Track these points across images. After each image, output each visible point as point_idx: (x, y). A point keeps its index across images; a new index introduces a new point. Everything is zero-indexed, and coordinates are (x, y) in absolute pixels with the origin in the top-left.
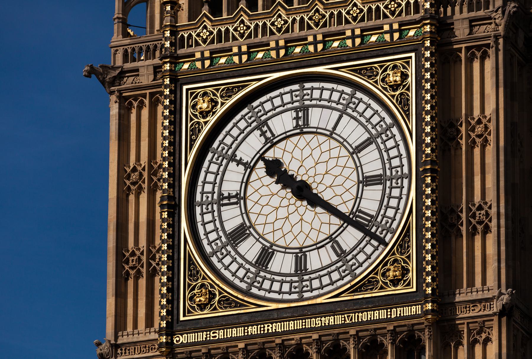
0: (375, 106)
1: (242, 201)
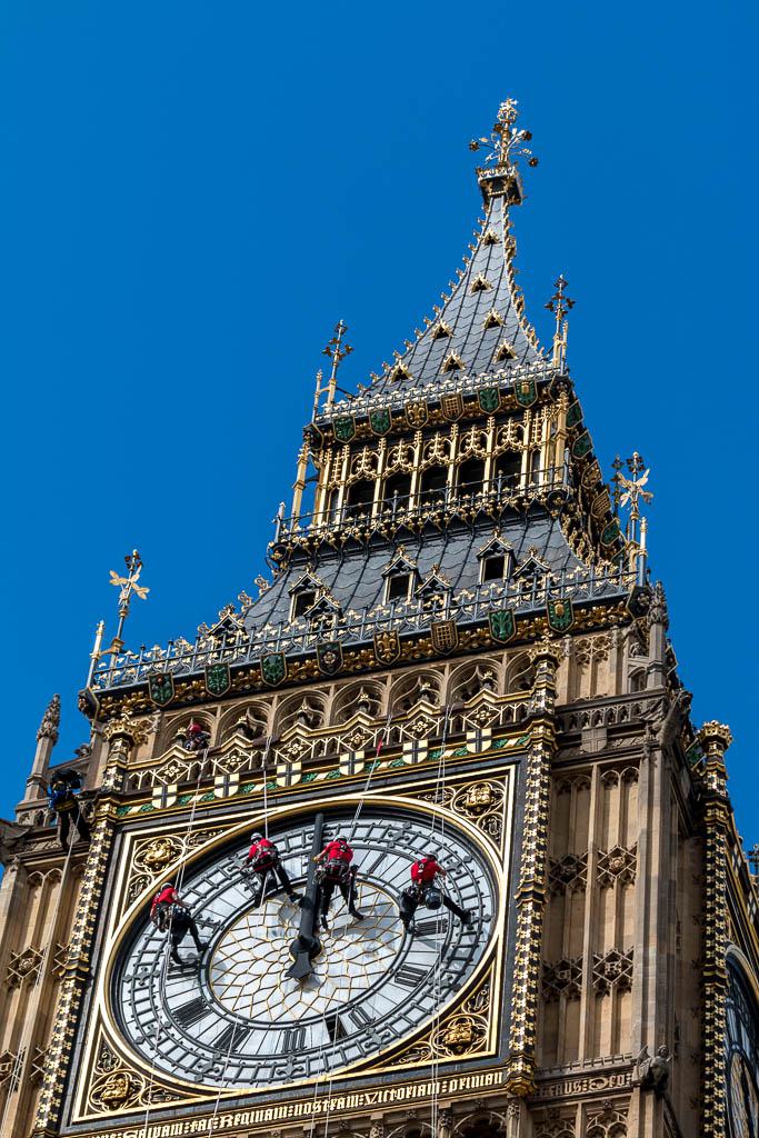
0: (440, 838)
1: (203, 971)
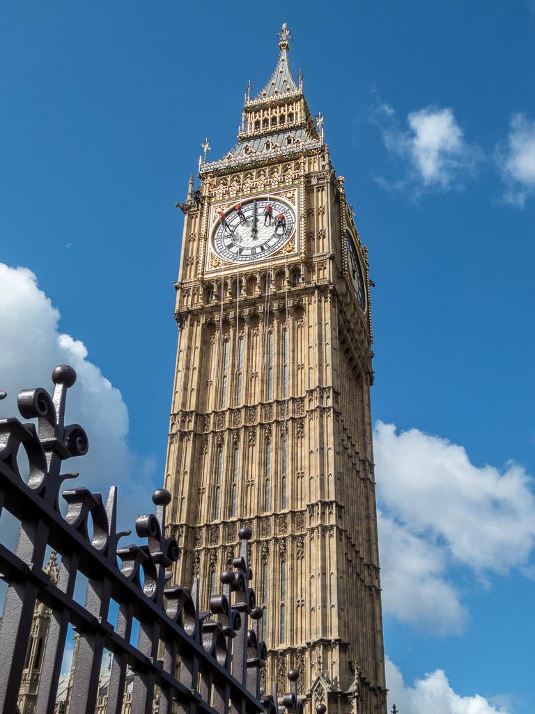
0: (282, 205)
